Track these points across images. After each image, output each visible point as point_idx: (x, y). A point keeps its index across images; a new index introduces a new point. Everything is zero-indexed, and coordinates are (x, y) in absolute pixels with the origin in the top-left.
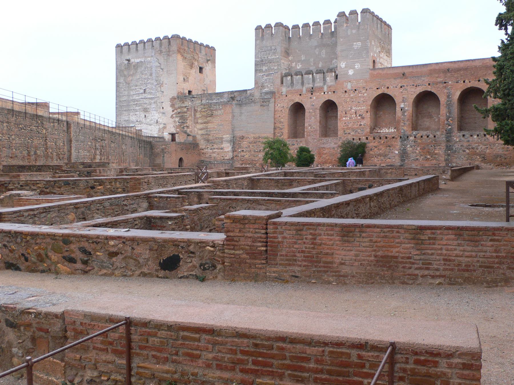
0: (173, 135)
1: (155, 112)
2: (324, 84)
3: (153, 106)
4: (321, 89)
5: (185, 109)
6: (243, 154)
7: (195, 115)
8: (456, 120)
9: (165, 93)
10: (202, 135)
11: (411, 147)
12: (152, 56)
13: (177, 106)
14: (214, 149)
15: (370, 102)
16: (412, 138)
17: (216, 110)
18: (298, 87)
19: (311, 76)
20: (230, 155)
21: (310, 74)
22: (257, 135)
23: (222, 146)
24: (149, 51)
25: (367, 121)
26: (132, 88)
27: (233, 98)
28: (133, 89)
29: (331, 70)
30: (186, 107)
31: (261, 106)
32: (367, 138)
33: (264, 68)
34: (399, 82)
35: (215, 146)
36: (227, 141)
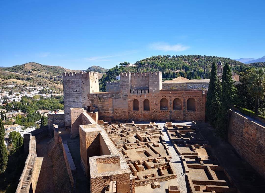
0: (89, 107)
1: (81, 99)
2: (145, 94)
3: (80, 96)
4: (144, 95)
5: (94, 98)
6: (117, 115)
7: (98, 101)
8: (186, 107)
9: (85, 92)
10: (101, 107)
11: (173, 114)
12: (79, 79)
13: (90, 97)
14: (106, 112)
15: (160, 100)
16: (173, 112)
17: (106, 99)
18: (136, 94)
19: (140, 91)
20: (112, 115)
21: (140, 90)
22: (122, 109)
23: (109, 112)
24: (78, 77)
25: (159, 106)
26: (71, 89)
27: (113, 96)
28: (72, 90)
29: (147, 90)
30: (93, 98)
31: (123, 99)
32: (159, 111)
33: (124, 87)
34: (169, 95)
35: (106, 112)
36: (111, 110)
